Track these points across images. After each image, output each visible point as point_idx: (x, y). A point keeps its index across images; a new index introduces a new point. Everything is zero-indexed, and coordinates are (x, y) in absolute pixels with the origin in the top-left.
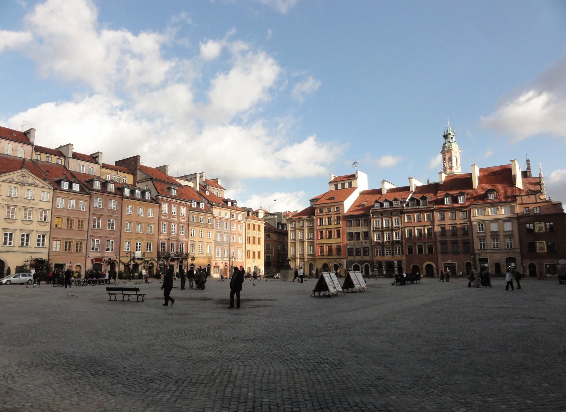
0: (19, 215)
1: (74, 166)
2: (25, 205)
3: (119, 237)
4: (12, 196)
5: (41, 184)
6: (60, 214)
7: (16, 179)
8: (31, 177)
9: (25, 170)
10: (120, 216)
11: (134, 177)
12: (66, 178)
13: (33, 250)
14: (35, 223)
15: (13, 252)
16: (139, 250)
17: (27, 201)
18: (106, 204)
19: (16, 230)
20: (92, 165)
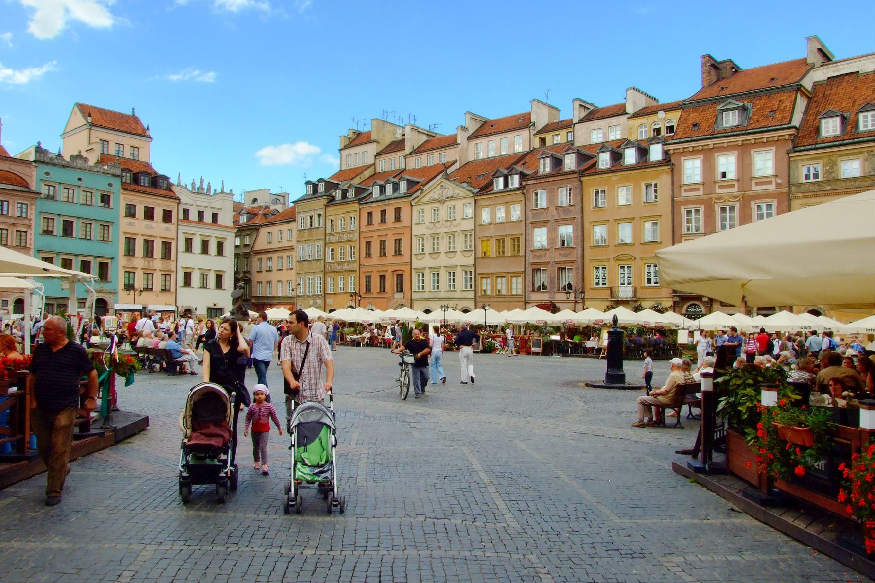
0: (443, 246)
2: (447, 230)
3: (580, 260)
5: (462, 194)
6: (486, 234)
7: (436, 197)
10: (579, 216)
13: (458, 295)
14: (459, 253)
15: (440, 299)
17: (449, 223)
19: (440, 267)
20: (614, 120)
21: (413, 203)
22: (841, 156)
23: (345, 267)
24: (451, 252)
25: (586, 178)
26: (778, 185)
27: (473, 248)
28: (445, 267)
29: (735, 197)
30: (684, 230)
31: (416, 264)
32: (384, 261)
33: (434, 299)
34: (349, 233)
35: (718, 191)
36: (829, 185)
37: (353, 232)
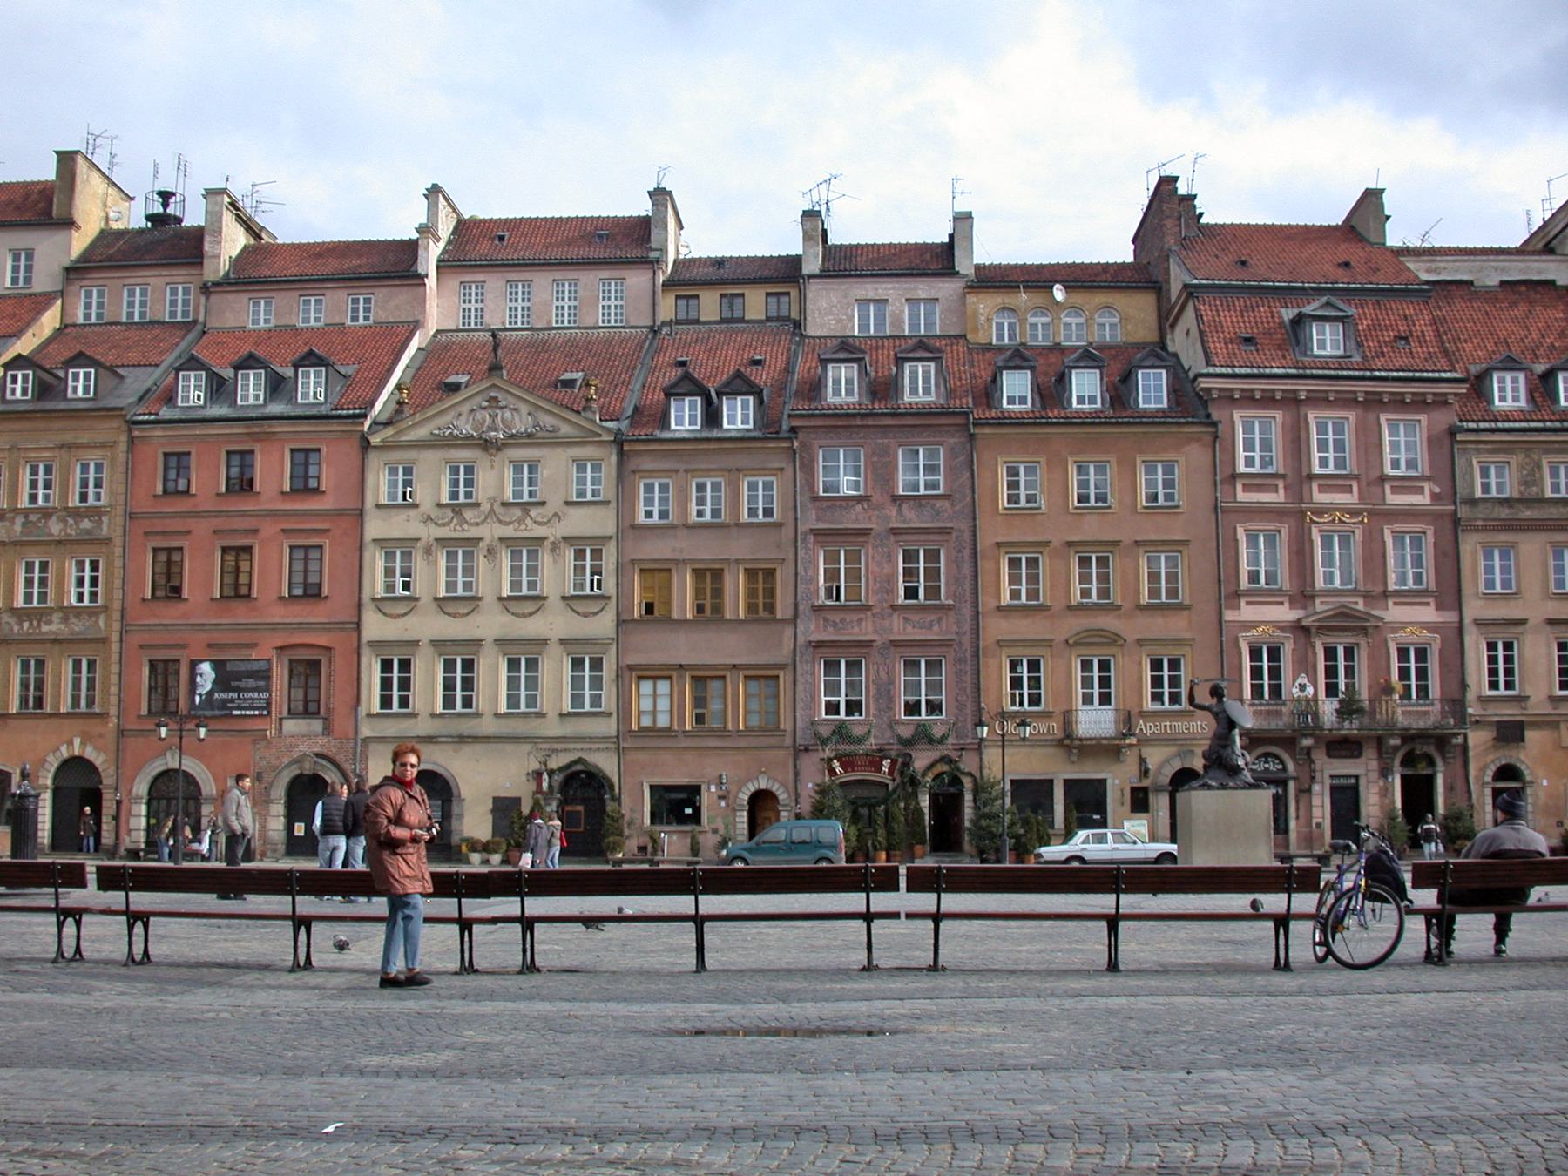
1: (832, 311)
2: (509, 532)
3: (966, 640)
4: (526, 498)
5: (565, 429)
7: (466, 427)
8: (524, 409)
9: (496, 381)
10: (964, 525)
11: (1159, 300)
12: (687, 377)
13: (553, 728)
15: (477, 739)
16: (1105, 699)
17: (517, 512)
18: (882, 473)
20: (923, 288)
21: (375, 440)
22: (1547, 452)
23: (54, 627)
24: (526, 601)
25: (987, 430)
26: (1434, 496)
27: (610, 586)
28: (499, 642)
29: (1354, 513)
30: (1244, 583)
31: (375, 626)
32: (240, 613)
33: (462, 739)
34: (77, 514)
35: (1320, 497)
36: (1528, 508)
37: (95, 513)
